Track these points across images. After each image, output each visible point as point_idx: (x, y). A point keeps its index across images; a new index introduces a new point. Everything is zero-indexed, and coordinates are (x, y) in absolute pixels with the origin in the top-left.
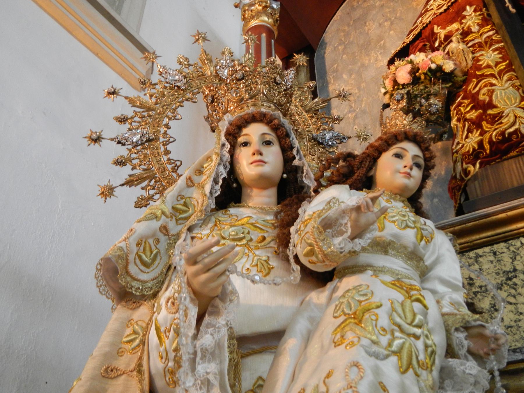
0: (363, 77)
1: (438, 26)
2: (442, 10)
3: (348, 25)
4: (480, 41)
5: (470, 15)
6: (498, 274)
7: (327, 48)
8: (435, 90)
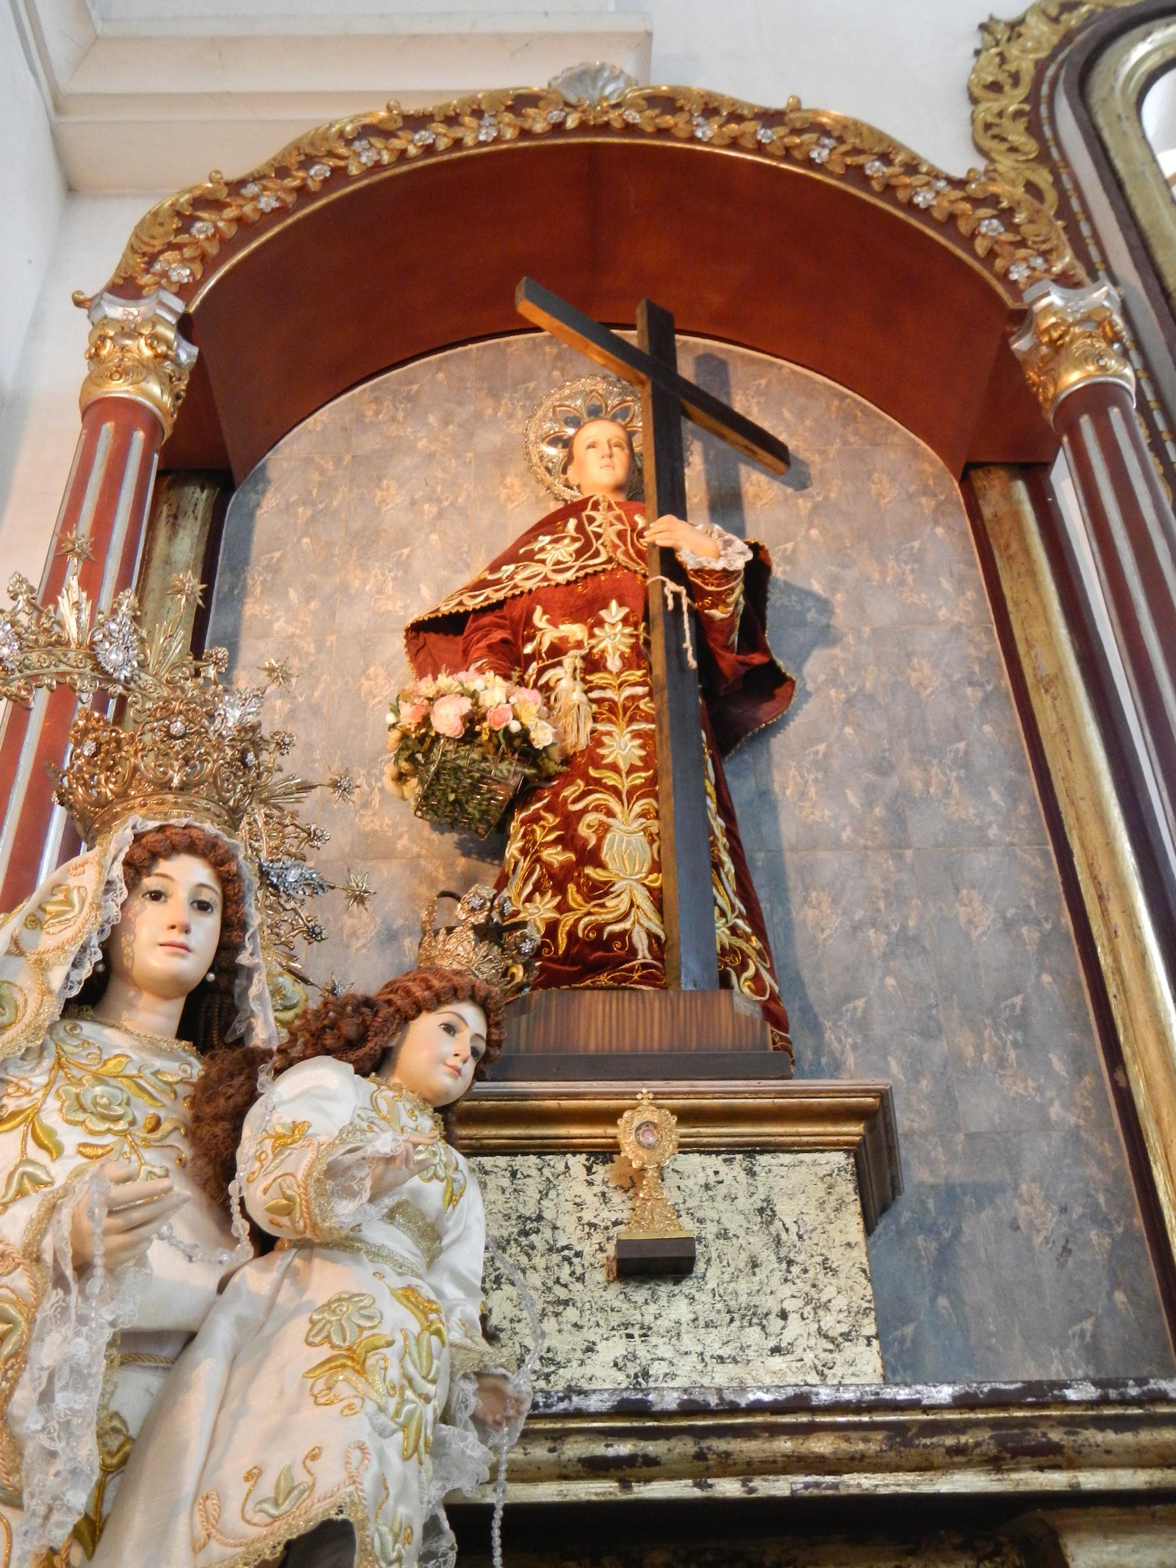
0: (337, 620)
1: (545, 613)
2: (562, 578)
3: (338, 461)
4: (616, 699)
5: (613, 625)
6: (507, 1217)
7: (269, 495)
8: (501, 772)
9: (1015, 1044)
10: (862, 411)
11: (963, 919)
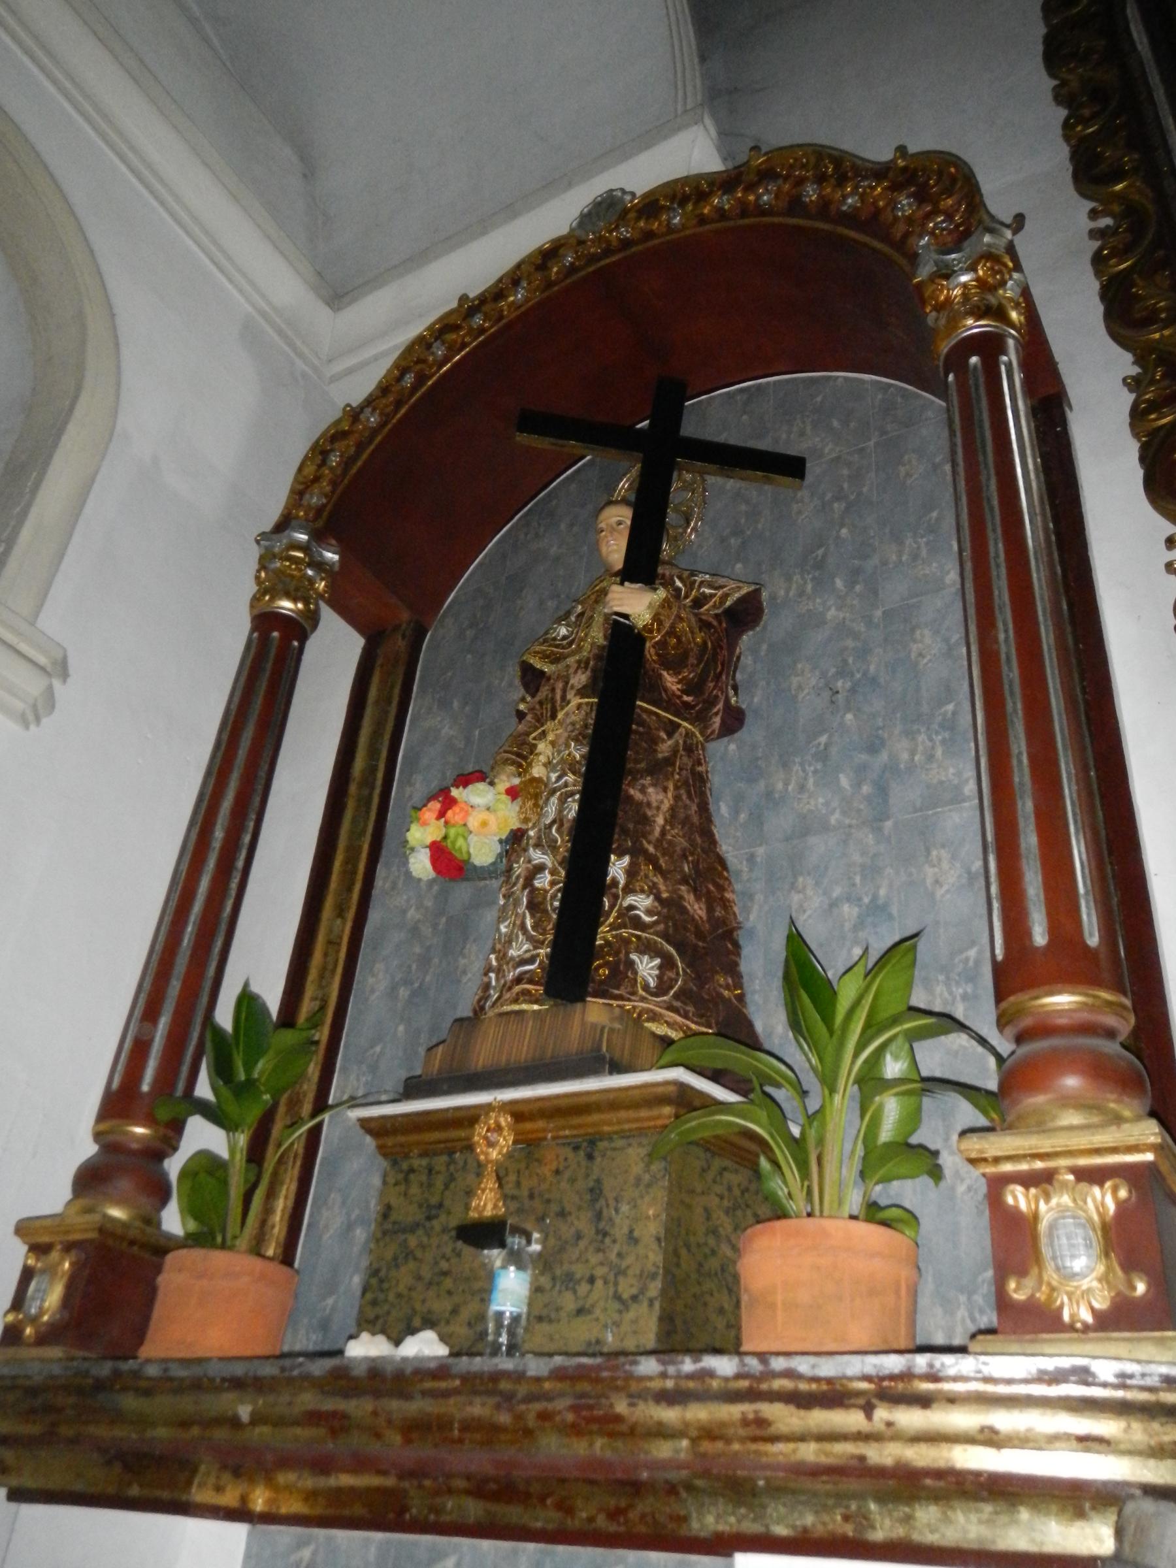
6: (420, 1206)
9: (965, 997)
10: (903, 397)
11: (929, 882)
